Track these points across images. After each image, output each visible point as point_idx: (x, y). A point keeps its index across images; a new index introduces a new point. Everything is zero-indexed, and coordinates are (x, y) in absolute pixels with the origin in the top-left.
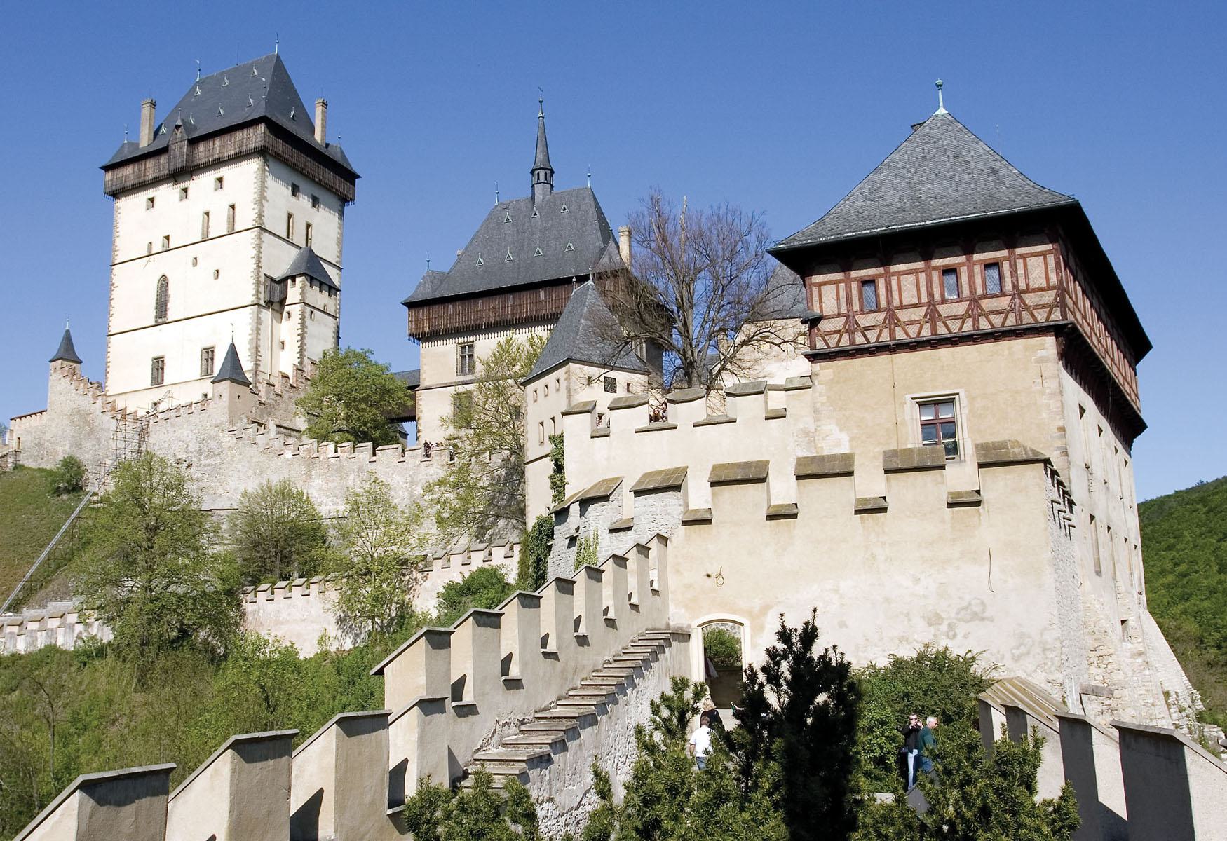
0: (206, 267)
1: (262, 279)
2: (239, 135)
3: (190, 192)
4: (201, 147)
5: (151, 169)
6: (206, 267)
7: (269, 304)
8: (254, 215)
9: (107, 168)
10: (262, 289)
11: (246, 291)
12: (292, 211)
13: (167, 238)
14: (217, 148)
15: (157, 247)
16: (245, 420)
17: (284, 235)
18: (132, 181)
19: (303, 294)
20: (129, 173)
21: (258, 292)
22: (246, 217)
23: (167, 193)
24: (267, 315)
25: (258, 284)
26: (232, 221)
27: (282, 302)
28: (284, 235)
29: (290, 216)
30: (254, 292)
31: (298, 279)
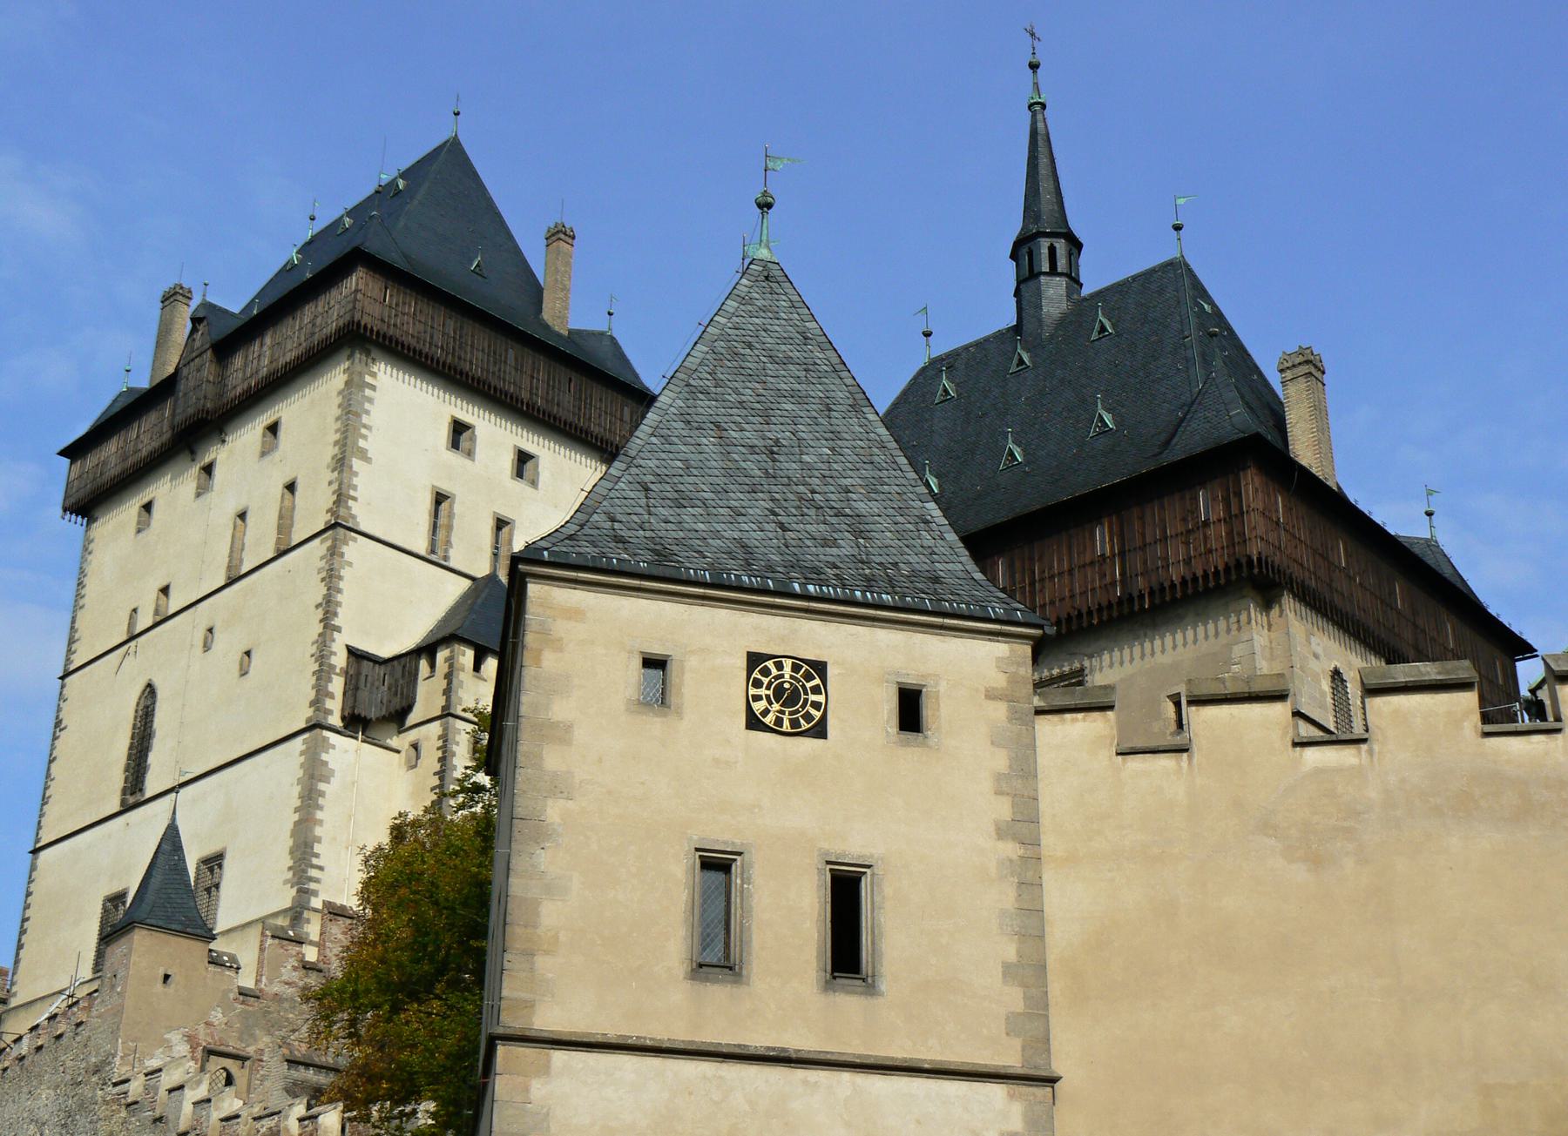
0: (228, 646)
1: (340, 660)
2: (308, 313)
3: (218, 472)
4: (238, 361)
5: (147, 435)
6: (228, 646)
7: (355, 723)
8: (328, 499)
9: (74, 452)
10: (337, 685)
11: (289, 690)
12: (445, 487)
13: (165, 590)
14: (264, 355)
15: (145, 620)
16: (182, 1049)
17: (421, 547)
18: (114, 468)
19: (447, 692)
20: (111, 455)
21: (321, 694)
22: (312, 513)
23: (172, 491)
24: (344, 751)
25: (323, 673)
26: (285, 521)
27: (398, 717)
28: (421, 547)
29: (440, 498)
30: (312, 695)
31: (442, 655)
